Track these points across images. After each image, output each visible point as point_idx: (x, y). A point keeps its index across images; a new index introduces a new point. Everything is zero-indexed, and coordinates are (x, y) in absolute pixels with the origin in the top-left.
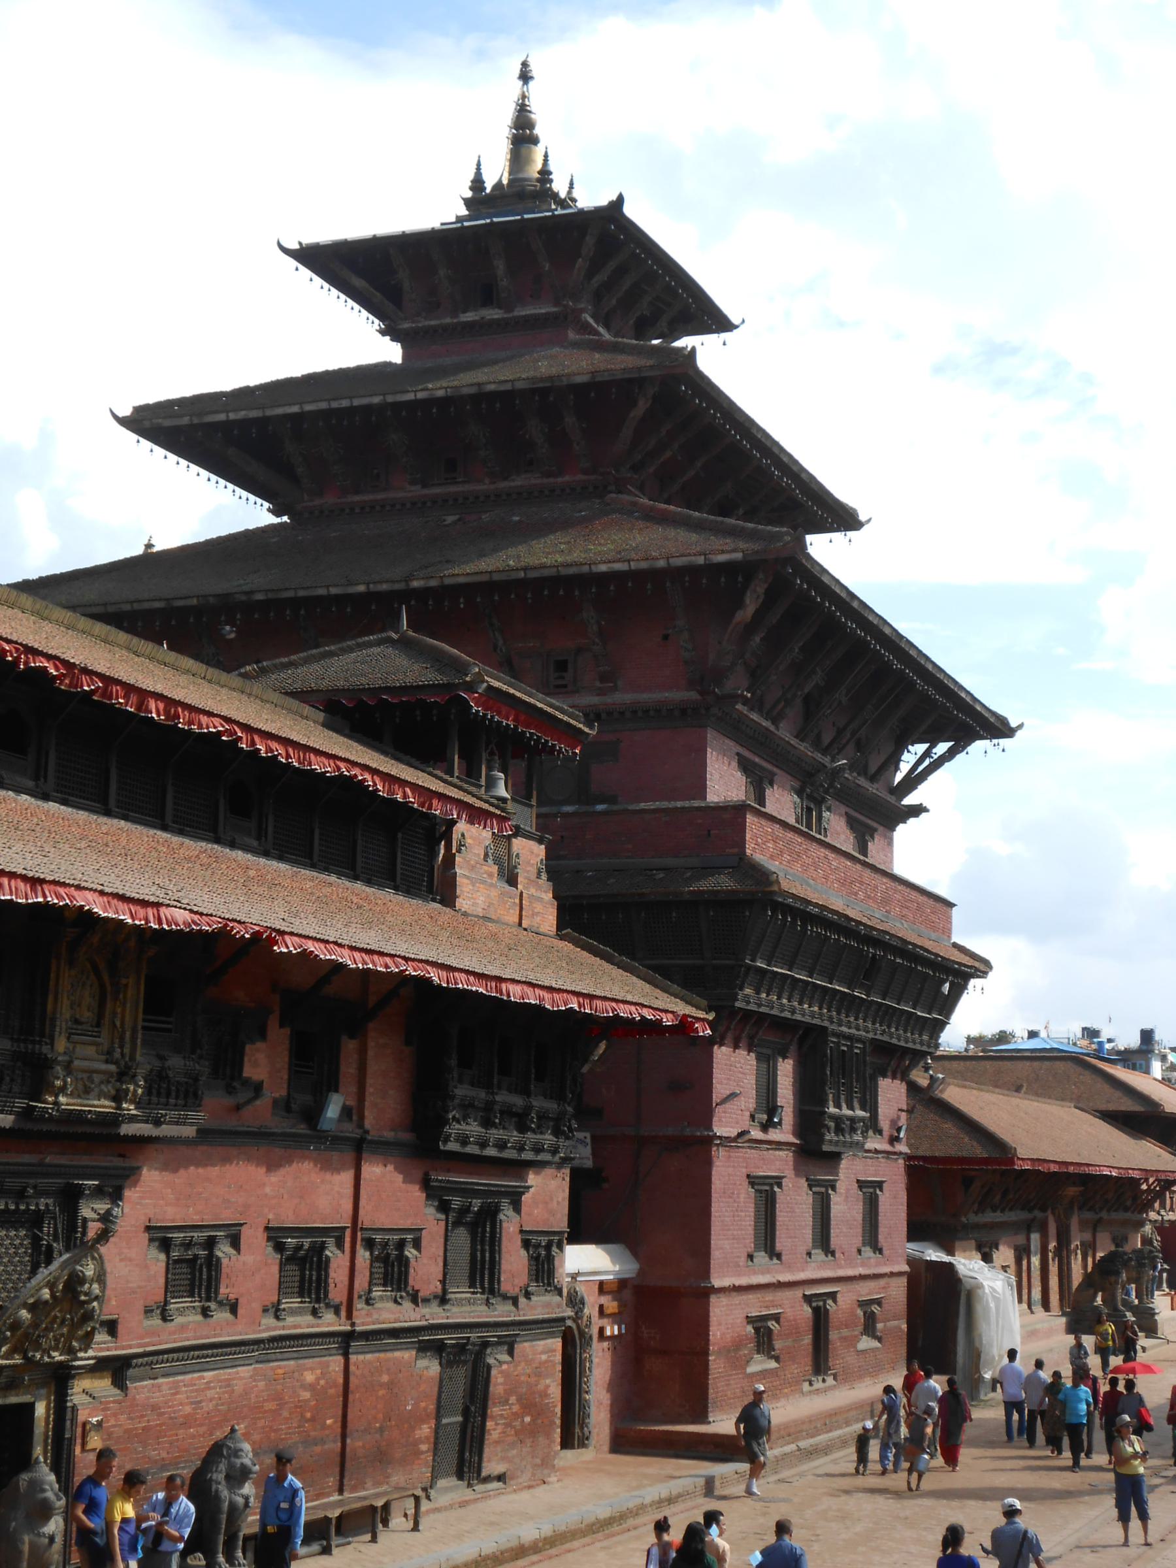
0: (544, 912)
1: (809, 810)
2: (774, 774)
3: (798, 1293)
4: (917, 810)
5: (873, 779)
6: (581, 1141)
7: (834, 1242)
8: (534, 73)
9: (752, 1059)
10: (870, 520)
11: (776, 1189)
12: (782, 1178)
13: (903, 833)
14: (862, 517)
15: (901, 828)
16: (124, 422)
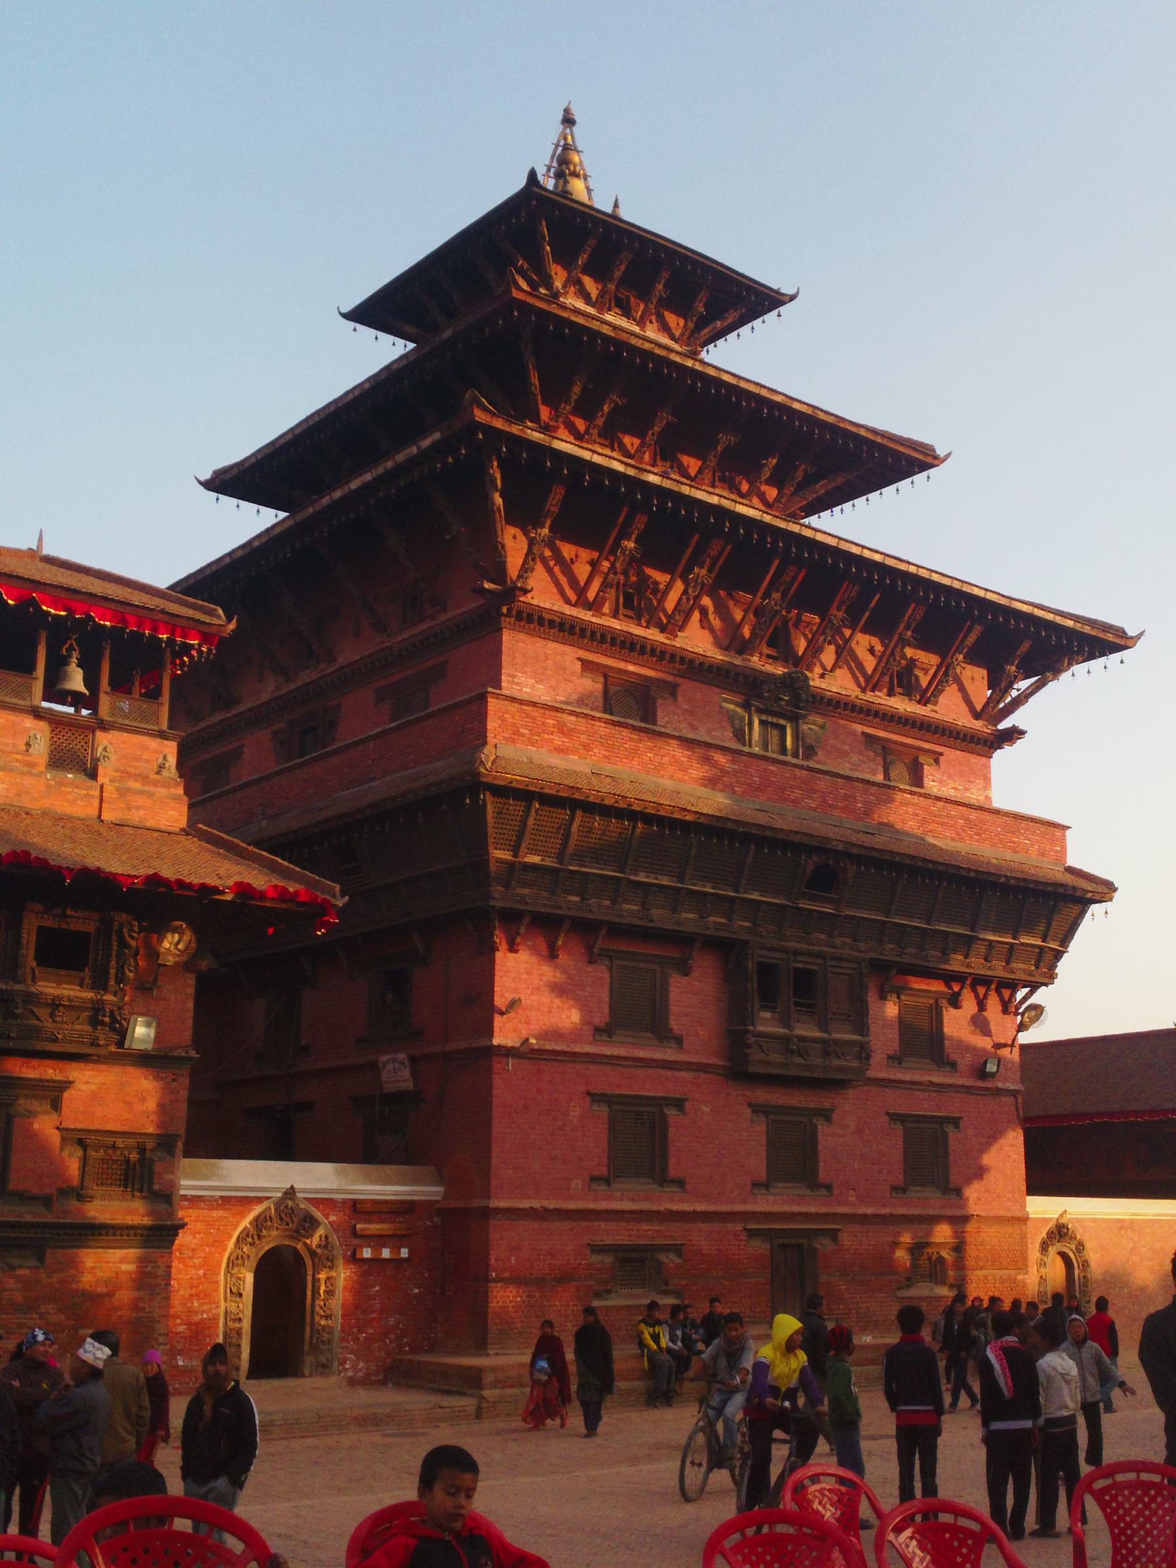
0: (168, 809)
1: (782, 729)
2: (676, 686)
3: (739, 1227)
4: (1013, 735)
5: (923, 701)
6: (402, 1063)
7: (823, 1175)
8: (576, 118)
9: (601, 972)
10: (949, 455)
11: (671, 1112)
12: (685, 1100)
13: (1002, 758)
14: (941, 452)
15: (998, 755)
16: (209, 485)
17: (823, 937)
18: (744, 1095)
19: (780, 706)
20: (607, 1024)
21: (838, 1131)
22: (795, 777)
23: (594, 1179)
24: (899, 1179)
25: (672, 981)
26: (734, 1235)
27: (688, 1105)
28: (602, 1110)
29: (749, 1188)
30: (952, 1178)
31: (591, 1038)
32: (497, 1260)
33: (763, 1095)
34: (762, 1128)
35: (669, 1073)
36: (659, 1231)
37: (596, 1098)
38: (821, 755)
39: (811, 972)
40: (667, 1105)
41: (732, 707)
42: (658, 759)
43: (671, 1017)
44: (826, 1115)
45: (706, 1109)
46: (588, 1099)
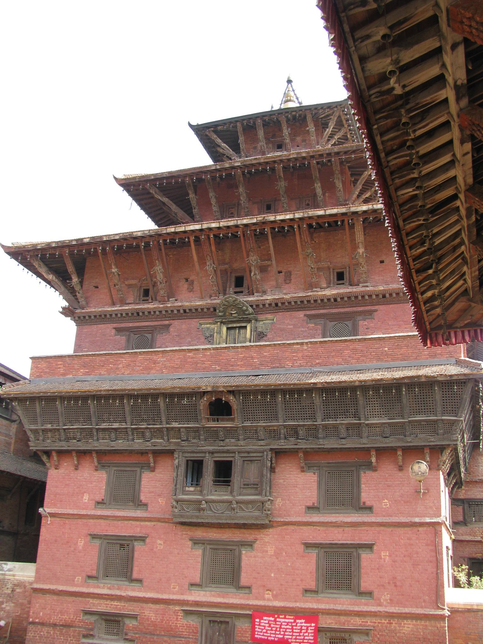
17: (233, 440)
18: (187, 534)
19: (235, 317)
20: (103, 500)
21: (259, 554)
22: (205, 356)
23: (90, 577)
24: (312, 585)
25: (144, 475)
26: (174, 613)
27: (148, 540)
28: (97, 542)
29: (186, 587)
30: (363, 584)
31: (93, 507)
32: (33, 613)
33: (200, 533)
34: (199, 552)
35: (138, 523)
36: (125, 606)
37: (94, 537)
38: (270, 336)
39: (231, 462)
40: (135, 540)
41: (208, 326)
42: (116, 366)
43: (142, 494)
44: (250, 545)
45: (159, 542)
46: (89, 537)
